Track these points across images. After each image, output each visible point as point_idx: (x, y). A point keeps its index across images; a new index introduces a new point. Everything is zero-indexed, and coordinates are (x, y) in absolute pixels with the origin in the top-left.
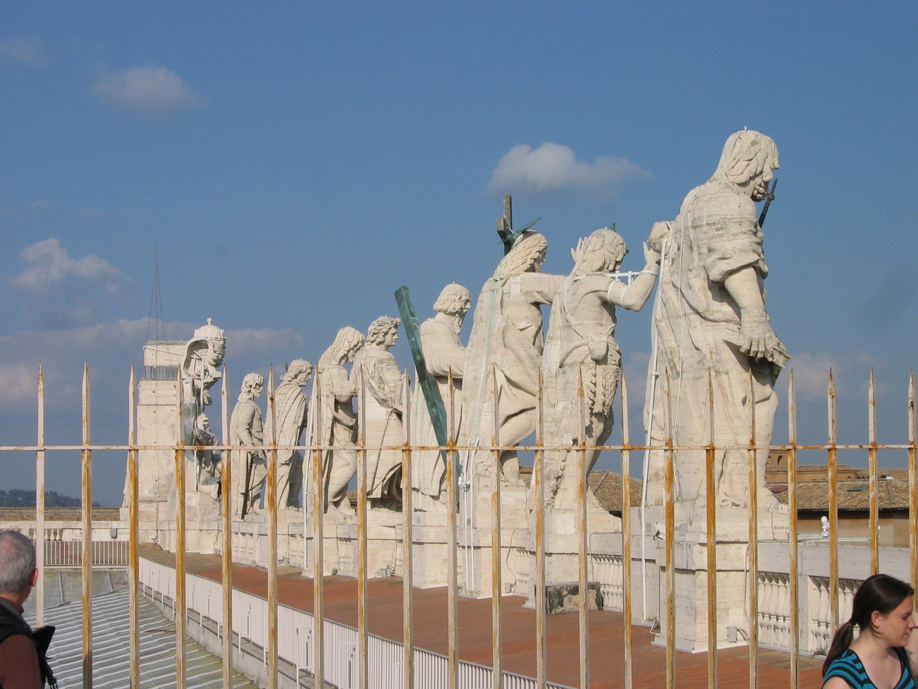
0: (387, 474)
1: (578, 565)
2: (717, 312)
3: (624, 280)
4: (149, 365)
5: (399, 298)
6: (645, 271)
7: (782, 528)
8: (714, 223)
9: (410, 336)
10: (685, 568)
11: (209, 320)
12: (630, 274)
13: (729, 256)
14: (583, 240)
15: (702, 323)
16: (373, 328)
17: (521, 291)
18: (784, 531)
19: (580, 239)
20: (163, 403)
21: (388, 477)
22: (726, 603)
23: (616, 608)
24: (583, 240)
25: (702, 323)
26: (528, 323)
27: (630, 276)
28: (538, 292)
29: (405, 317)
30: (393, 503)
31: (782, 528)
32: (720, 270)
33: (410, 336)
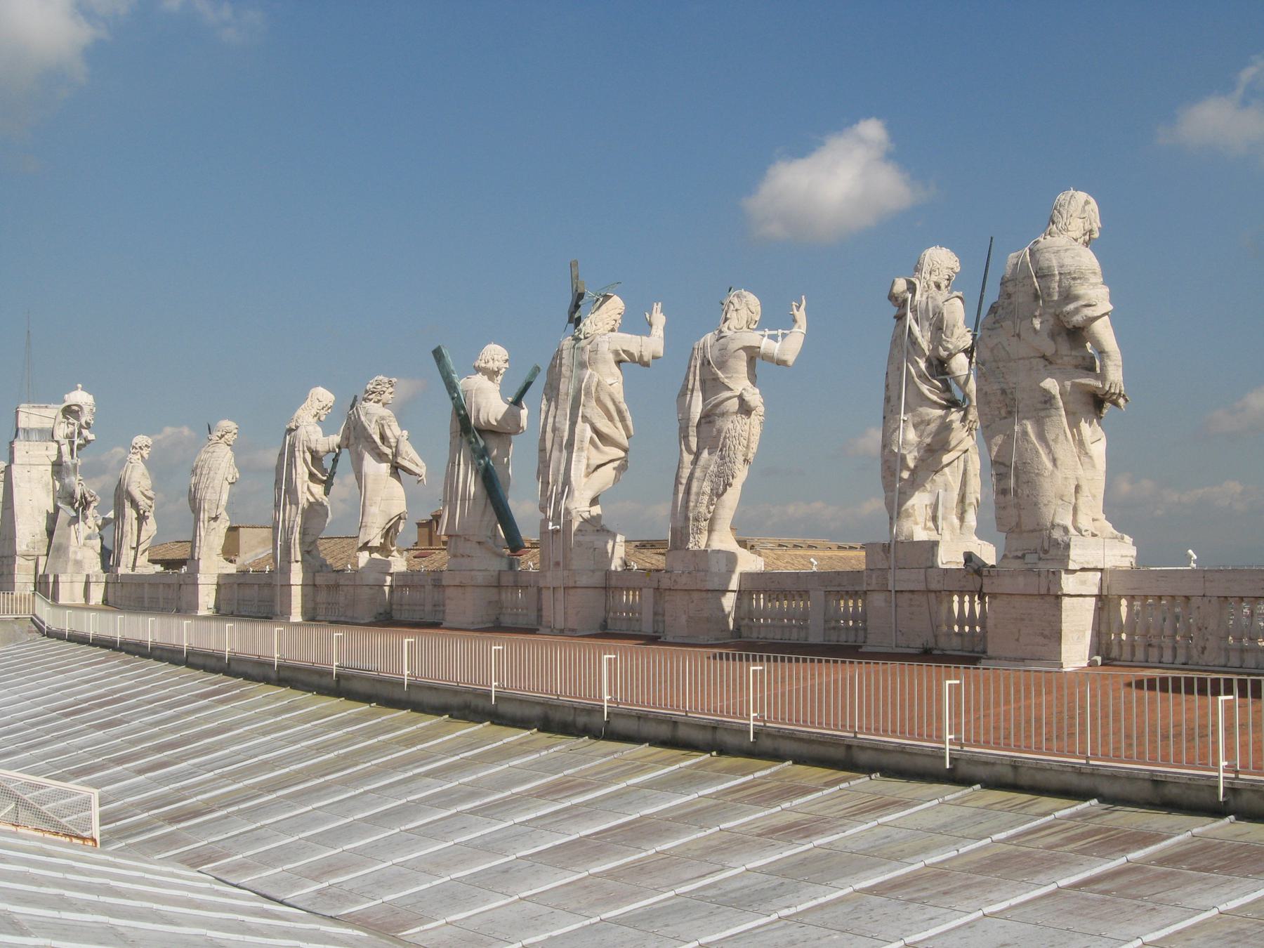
0: (387, 524)
1: (447, 611)
2: (1066, 356)
3: (774, 338)
4: (22, 426)
5: (438, 357)
6: (795, 329)
7: (1126, 556)
8: (1069, 273)
9: (452, 392)
10: (1043, 591)
11: (80, 386)
12: (780, 331)
13: (1094, 303)
14: (657, 305)
15: (1045, 366)
16: (372, 387)
17: (609, 349)
18: (1128, 559)
19: (655, 304)
20: (37, 463)
21: (387, 527)
22: (1083, 625)
23: (766, 639)
24: (657, 305)
25: (1045, 366)
26: (614, 379)
27: (780, 334)
28: (624, 351)
29: (446, 374)
30: (383, 551)
31: (1126, 556)
32: (1086, 316)
33: (452, 392)
